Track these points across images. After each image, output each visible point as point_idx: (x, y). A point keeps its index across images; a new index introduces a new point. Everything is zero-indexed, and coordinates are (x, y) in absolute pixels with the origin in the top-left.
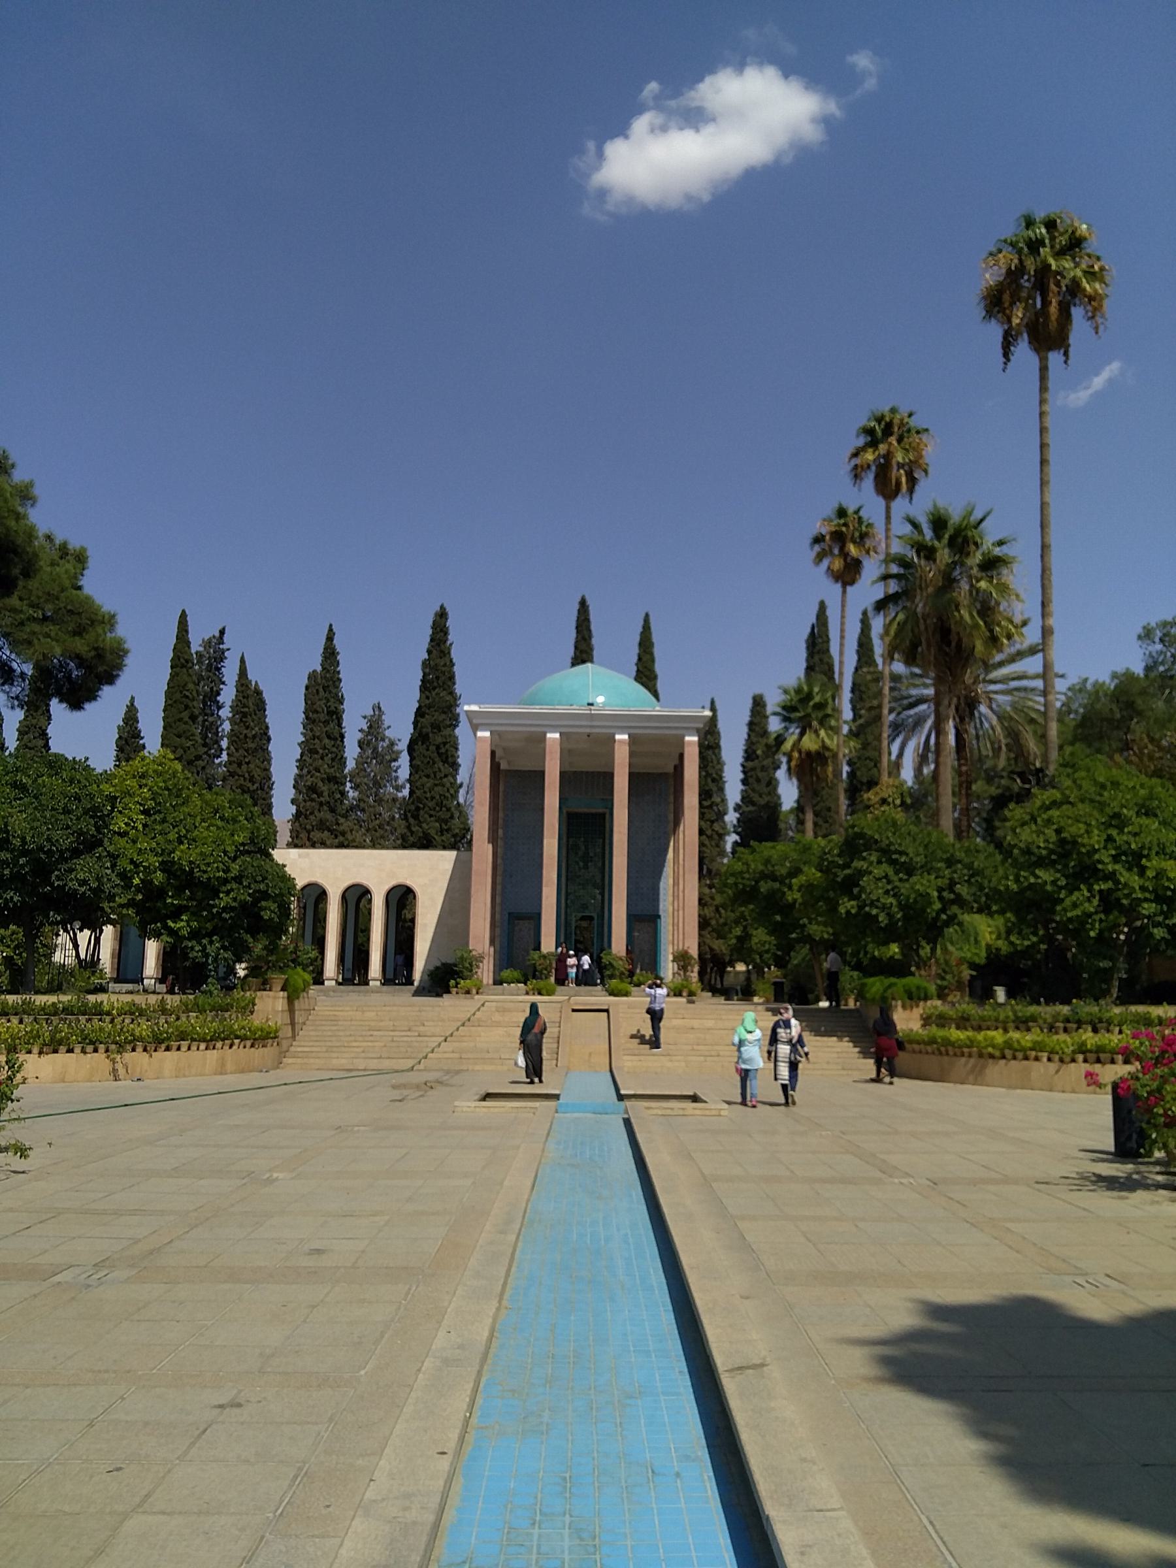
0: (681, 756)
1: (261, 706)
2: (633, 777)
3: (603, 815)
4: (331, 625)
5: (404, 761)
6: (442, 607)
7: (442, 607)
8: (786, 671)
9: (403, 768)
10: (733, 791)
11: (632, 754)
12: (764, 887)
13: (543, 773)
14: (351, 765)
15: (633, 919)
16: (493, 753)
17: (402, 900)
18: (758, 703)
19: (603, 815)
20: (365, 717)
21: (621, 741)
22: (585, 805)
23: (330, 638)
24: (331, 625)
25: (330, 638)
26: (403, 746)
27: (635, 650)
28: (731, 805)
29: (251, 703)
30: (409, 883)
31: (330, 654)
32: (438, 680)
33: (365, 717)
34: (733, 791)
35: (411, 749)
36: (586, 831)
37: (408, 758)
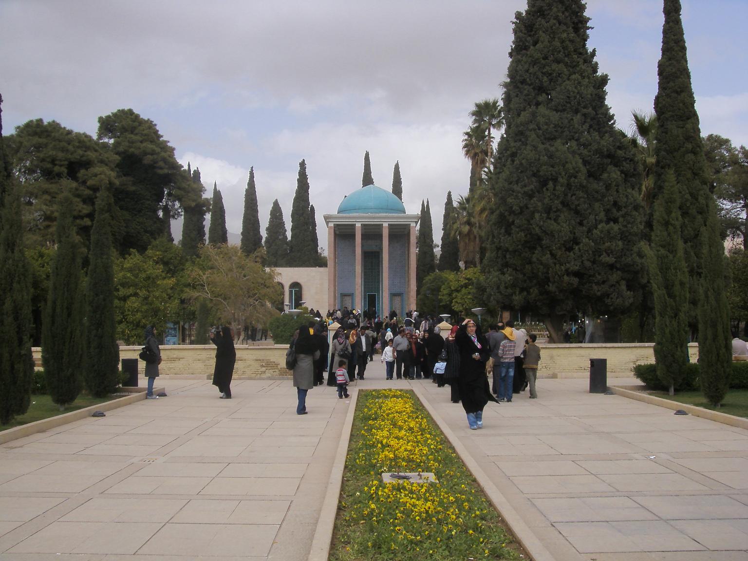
0: (410, 230)
15: (393, 295)
16: (334, 230)
17: (296, 287)
19: (378, 253)
21: (386, 227)
30: (298, 281)
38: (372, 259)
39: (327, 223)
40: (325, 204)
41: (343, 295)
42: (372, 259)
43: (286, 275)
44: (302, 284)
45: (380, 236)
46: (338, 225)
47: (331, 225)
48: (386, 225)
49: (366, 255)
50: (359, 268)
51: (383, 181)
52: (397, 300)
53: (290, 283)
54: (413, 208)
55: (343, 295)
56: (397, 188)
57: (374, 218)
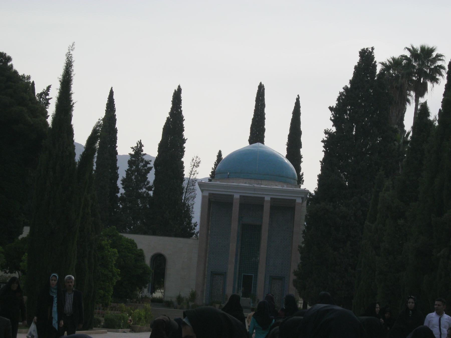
4: (112, 88)
5: (153, 171)
6: (179, 86)
7: (179, 86)
9: (151, 177)
14: (122, 173)
17: (159, 260)
20: (132, 148)
24: (112, 88)
26: (152, 164)
27: (291, 116)
30: (163, 252)
32: (174, 130)
33: (132, 148)
35: (156, 164)
37: (154, 170)
39: (202, 191)
41: (214, 274)
42: (250, 234)
43: (148, 245)
44: (167, 256)
47: (206, 194)
50: (233, 246)
53: (151, 254)
55: (214, 274)
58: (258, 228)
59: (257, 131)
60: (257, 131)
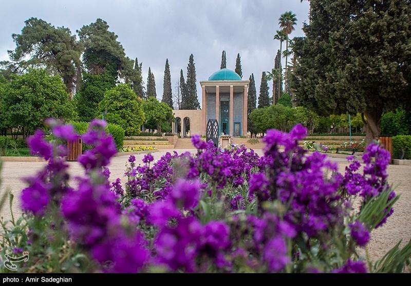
1: (153, 77)
2: (234, 93)
3: (228, 102)
6: (192, 55)
7: (192, 55)
8: (270, 67)
10: (258, 94)
11: (234, 89)
12: (258, 117)
13: (215, 93)
15: (235, 123)
17: (187, 120)
18: (264, 73)
22: (223, 99)
23: (167, 61)
25: (167, 61)
28: (257, 98)
29: (151, 77)
31: (167, 66)
34: (258, 94)
36: (225, 105)
38: (225, 105)
39: (202, 85)
40: (203, 76)
45: (229, 93)
46: (207, 87)
47: (204, 86)
48: (232, 86)
49: (222, 103)
50: (218, 109)
51: (231, 66)
52: (237, 126)
54: (245, 78)
56: (238, 70)
57: (225, 82)
58: (228, 102)
59: (223, 66)
60: (223, 66)
